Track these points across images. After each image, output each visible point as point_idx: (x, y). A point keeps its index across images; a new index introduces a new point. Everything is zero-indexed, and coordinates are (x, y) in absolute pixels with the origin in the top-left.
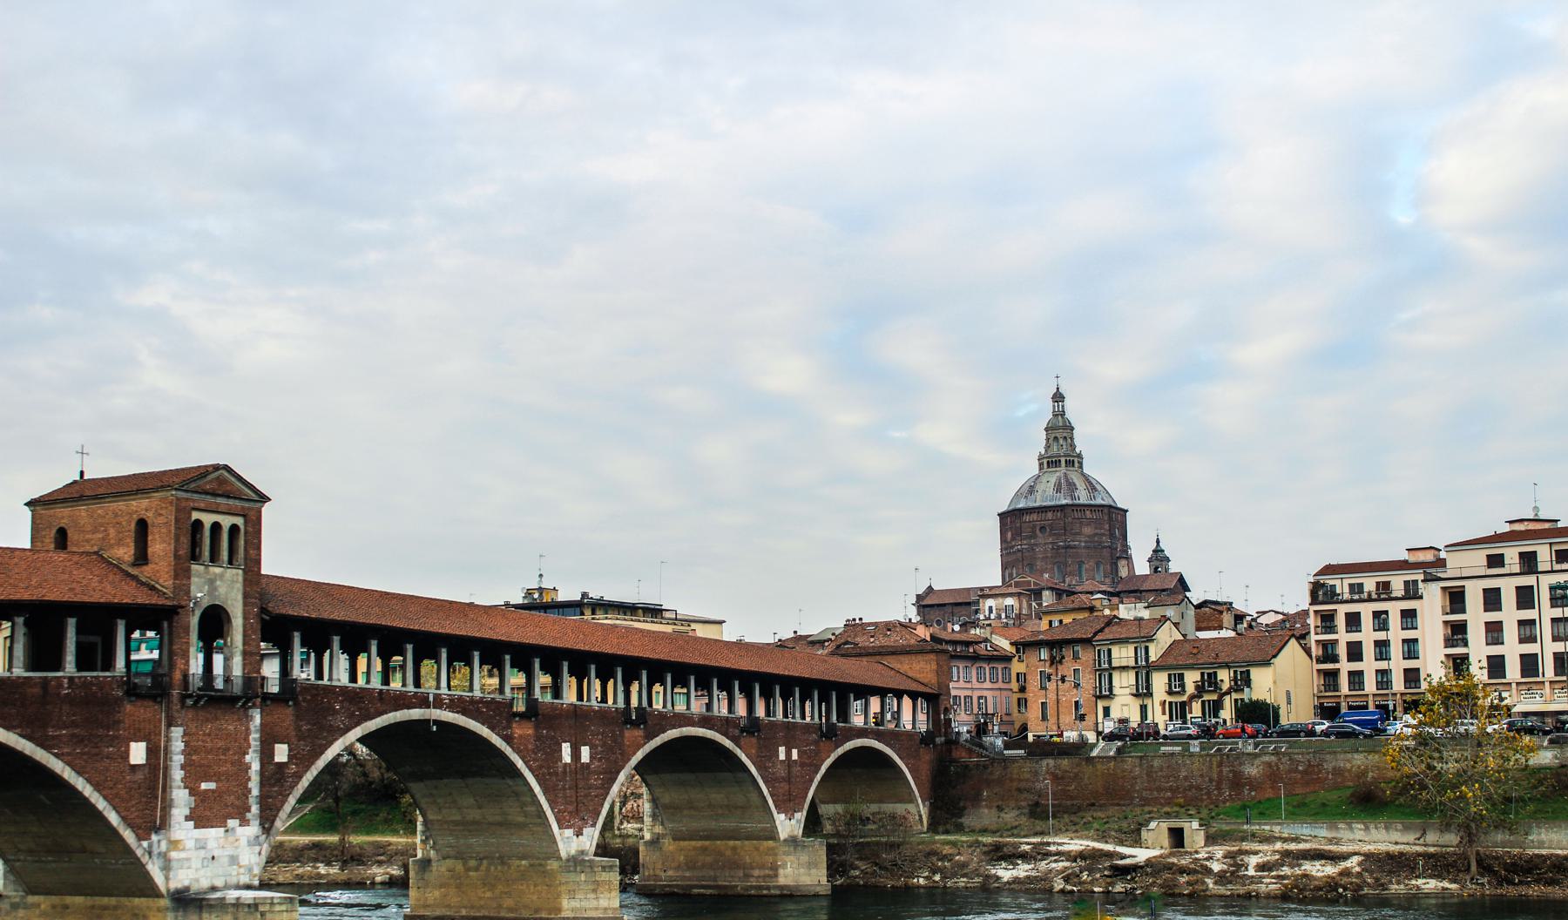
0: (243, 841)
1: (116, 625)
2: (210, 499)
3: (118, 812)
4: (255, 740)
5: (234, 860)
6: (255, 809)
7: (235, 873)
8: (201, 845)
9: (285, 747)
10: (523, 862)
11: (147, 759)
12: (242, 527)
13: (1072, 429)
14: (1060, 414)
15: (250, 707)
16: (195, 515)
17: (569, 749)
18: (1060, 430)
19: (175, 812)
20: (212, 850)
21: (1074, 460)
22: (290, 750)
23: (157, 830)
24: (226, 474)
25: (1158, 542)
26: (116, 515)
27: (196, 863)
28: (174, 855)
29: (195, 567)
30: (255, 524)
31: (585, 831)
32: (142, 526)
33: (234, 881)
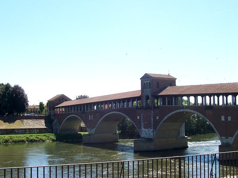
0: (151, 131)
5: (149, 134)
8: (145, 131)
16: (144, 82)
17: (224, 117)
31: (229, 138)
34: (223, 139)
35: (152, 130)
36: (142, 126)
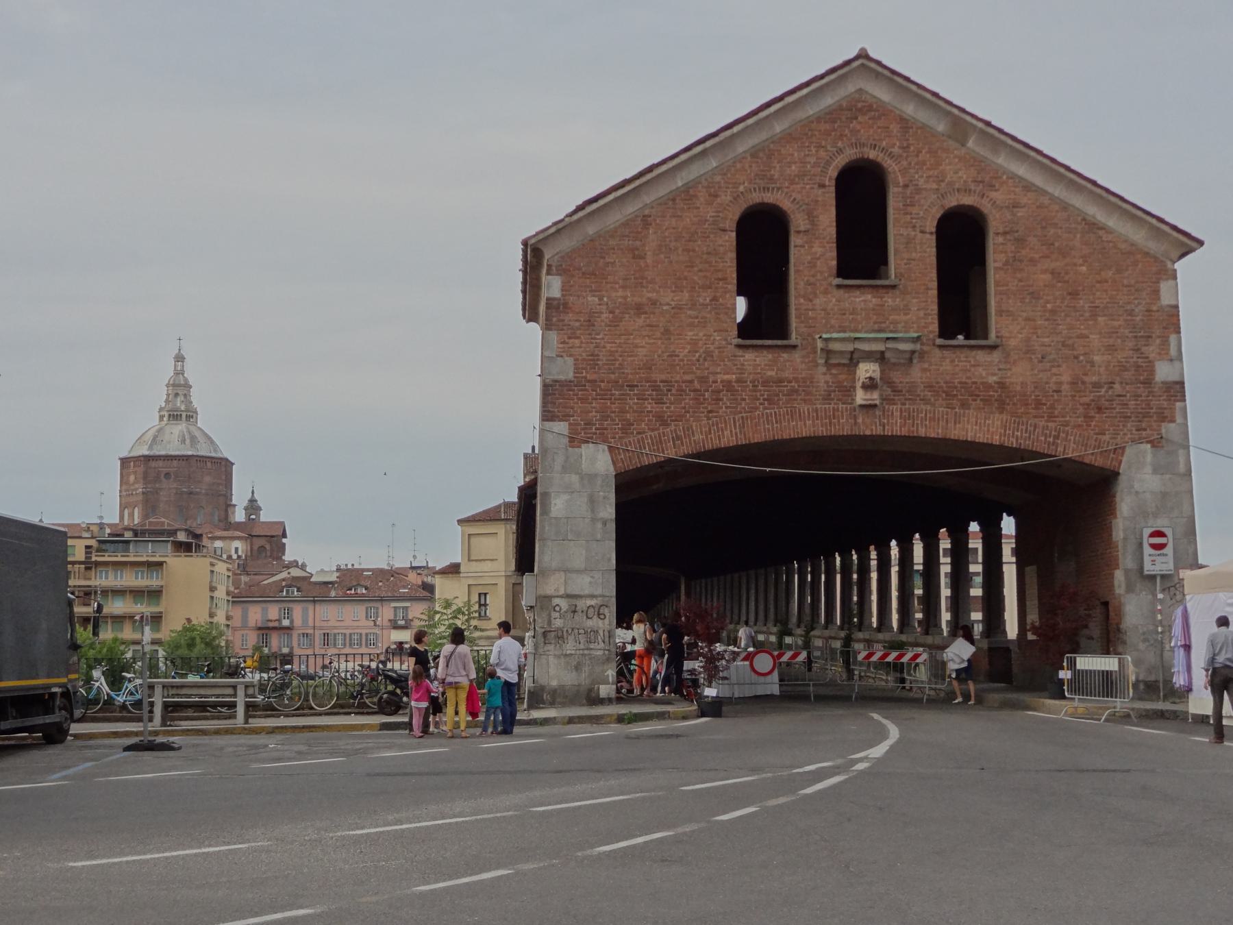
13: (191, 387)
14: (179, 373)
18: (180, 387)
21: (191, 415)
25: (253, 492)
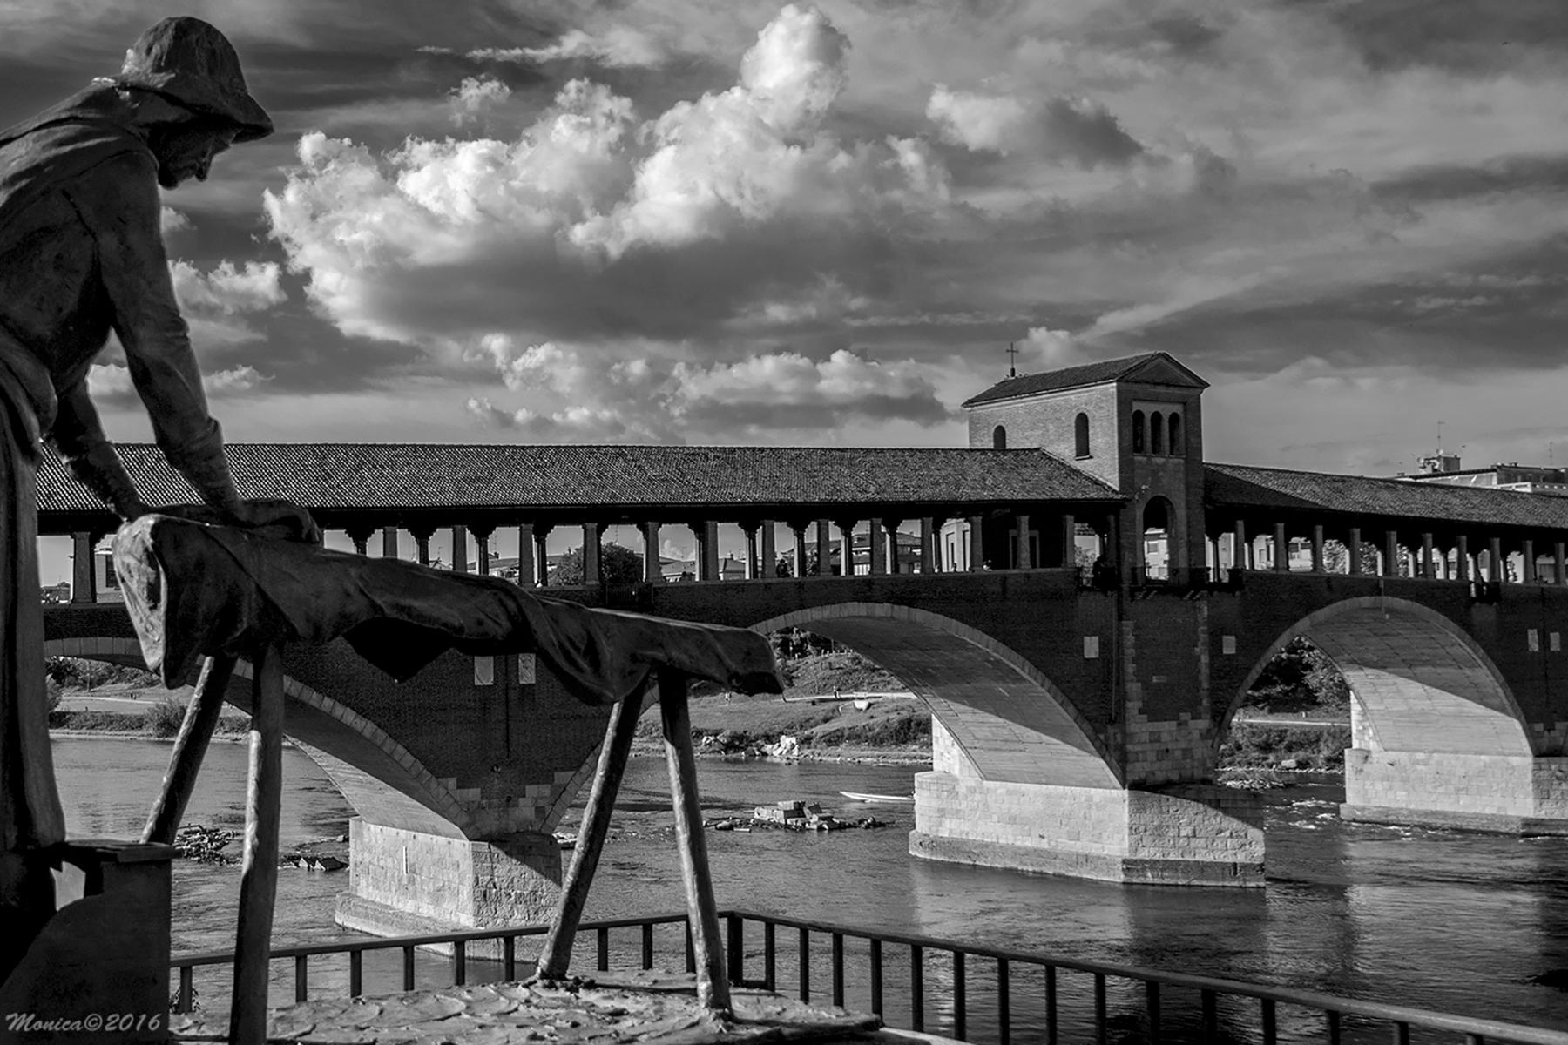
0: (1196, 735)
1: (1065, 520)
2: (1151, 389)
3: (1075, 705)
4: (1203, 631)
5: (1187, 752)
6: (1205, 702)
7: (1188, 767)
8: (1155, 738)
9: (1233, 638)
10: (1483, 757)
11: (1100, 653)
12: (1181, 415)
15: (1198, 599)
16: (1137, 406)
17: (1537, 637)
19: (1129, 704)
20: (1166, 742)
22: (1238, 642)
23: (1112, 722)
24: (1164, 361)
26: (1055, 411)
27: (1152, 756)
28: (1130, 747)
29: (1139, 458)
30: (1193, 409)
32: (1082, 422)
33: (1188, 773)
34: (1538, 732)
35: (1204, 724)
36: (1133, 706)
